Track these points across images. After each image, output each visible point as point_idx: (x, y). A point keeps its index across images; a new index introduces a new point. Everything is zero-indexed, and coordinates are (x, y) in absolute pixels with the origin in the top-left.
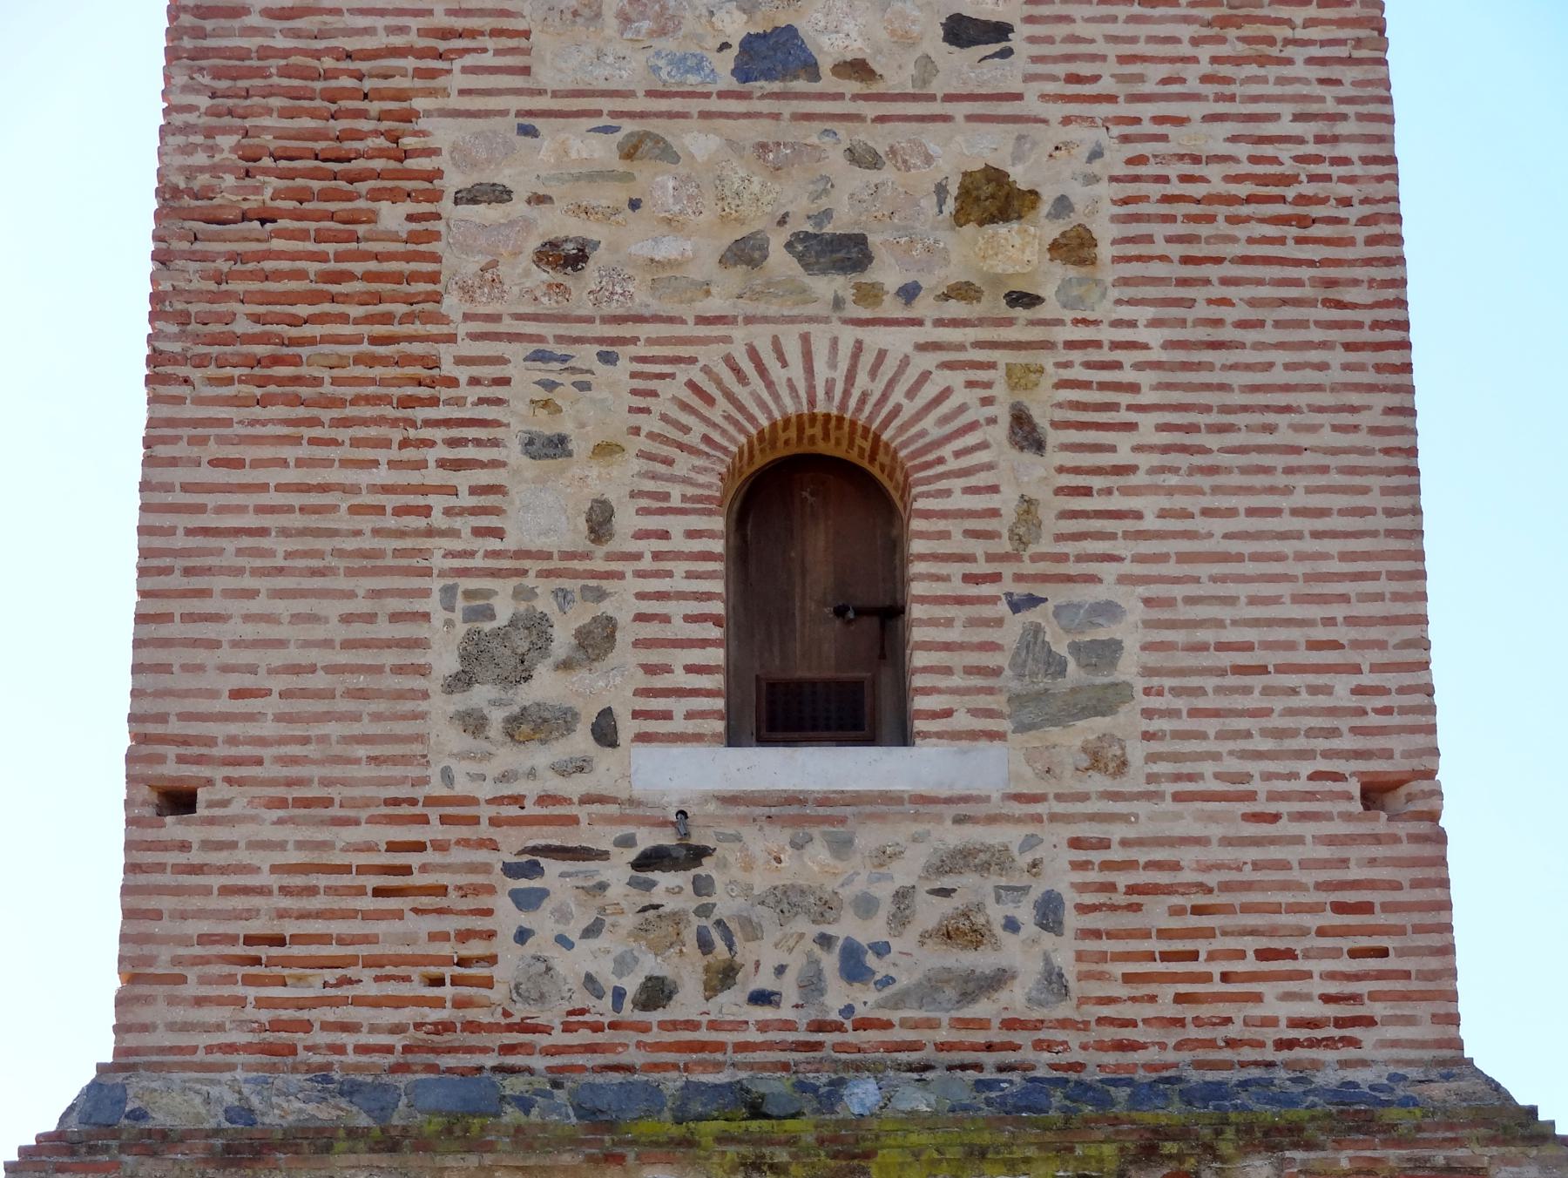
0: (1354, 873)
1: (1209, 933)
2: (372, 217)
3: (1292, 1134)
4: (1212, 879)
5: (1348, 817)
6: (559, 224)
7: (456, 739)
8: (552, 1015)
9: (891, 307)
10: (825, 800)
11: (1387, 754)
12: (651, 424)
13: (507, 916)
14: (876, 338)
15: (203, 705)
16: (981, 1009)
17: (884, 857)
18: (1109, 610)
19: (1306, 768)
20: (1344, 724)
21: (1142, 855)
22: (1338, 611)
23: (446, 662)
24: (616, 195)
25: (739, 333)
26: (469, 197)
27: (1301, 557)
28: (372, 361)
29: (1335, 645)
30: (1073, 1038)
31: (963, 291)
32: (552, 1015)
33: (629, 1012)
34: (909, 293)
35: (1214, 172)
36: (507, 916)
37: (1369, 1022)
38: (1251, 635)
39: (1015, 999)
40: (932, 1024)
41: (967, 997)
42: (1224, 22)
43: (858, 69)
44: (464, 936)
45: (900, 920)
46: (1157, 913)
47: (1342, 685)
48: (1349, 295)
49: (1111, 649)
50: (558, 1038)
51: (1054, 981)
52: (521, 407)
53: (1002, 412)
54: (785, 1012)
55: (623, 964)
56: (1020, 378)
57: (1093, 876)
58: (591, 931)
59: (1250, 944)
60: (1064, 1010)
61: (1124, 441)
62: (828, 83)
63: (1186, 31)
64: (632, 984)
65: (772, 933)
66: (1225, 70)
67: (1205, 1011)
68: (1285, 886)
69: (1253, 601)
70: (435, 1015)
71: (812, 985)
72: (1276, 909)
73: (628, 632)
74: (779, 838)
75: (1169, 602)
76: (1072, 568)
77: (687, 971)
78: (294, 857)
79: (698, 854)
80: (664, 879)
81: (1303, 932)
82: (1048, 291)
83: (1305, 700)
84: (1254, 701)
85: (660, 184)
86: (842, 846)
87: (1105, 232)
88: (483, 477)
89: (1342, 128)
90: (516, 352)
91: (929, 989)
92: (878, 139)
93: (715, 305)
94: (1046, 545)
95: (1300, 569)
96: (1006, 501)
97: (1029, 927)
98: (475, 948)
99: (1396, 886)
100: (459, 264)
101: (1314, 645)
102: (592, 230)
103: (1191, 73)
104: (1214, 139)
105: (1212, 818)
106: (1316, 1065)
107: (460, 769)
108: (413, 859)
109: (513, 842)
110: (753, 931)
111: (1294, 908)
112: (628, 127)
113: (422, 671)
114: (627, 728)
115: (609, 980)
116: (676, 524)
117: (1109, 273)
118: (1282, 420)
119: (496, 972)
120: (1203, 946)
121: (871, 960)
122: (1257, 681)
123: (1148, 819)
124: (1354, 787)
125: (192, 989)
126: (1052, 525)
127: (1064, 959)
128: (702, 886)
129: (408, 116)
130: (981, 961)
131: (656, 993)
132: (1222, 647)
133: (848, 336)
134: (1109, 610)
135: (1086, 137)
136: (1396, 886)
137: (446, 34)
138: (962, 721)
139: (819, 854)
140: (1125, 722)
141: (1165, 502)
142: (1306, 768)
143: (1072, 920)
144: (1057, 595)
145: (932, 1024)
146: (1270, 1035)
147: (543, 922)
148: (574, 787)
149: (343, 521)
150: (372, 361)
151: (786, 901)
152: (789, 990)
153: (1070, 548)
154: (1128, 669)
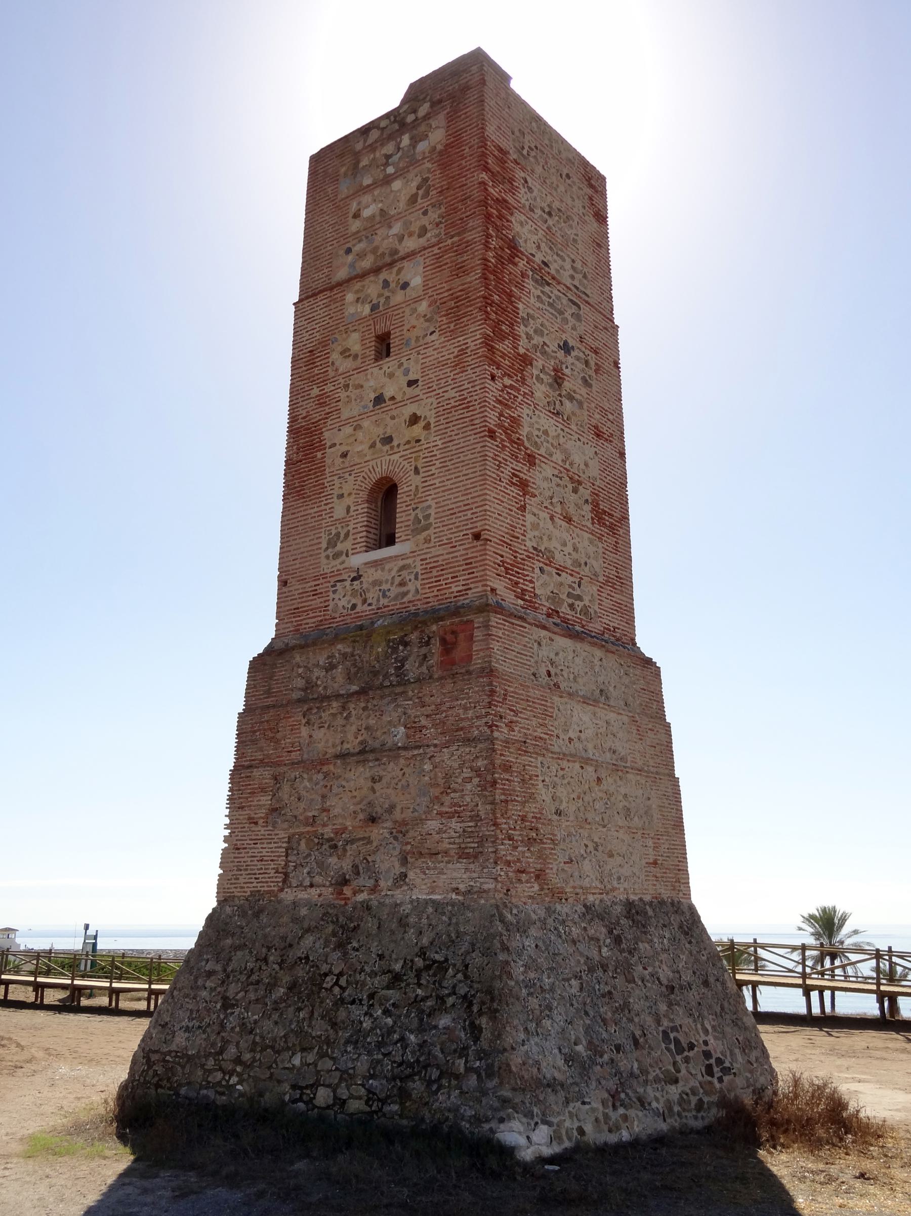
0: (470, 556)
1: (443, 575)
2: (316, 456)
3: (442, 619)
4: (444, 563)
5: (469, 543)
6: (344, 448)
7: (324, 561)
8: (337, 615)
9: (396, 450)
10: (381, 560)
11: (476, 527)
12: (356, 487)
13: (332, 596)
14: (392, 458)
15: (288, 564)
16: (405, 599)
17: (390, 570)
18: (429, 507)
19: (462, 534)
20: (469, 522)
21: (432, 560)
22: (470, 496)
23: (324, 545)
24: (352, 439)
25: (370, 463)
26: (330, 447)
27: (463, 486)
28: (315, 486)
29: (468, 504)
30: (419, 603)
31: (408, 442)
32: (337, 615)
33: (350, 612)
34: (399, 446)
35: (452, 401)
36: (332, 596)
37: (470, 589)
38: (454, 506)
39: (410, 597)
40: (396, 605)
41: (403, 598)
42: (456, 365)
43: (393, 398)
44: (325, 601)
45: (392, 584)
46: (435, 573)
47: (469, 513)
48: (476, 422)
49: (427, 517)
50: (338, 619)
51: (417, 591)
52: (336, 489)
53: (413, 468)
54: (373, 607)
55: (349, 602)
56: (416, 459)
57: (424, 567)
58: (344, 596)
59: (450, 576)
60: (419, 597)
61: (433, 468)
62: (388, 403)
63: (448, 370)
64: (349, 606)
65: (372, 590)
66: (456, 377)
67: (442, 592)
68: (457, 561)
69: (455, 498)
70: (320, 619)
71: (378, 600)
72: (455, 567)
73: (352, 532)
74: (373, 570)
75: (439, 502)
76: (423, 499)
77: (358, 601)
78: (301, 591)
79: (360, 576)
80: (355, 583)
81: (459, 571)
82: (422, 438)
83: (463, 518)
84: (453, 521)
85: (360, 435)
86: (383, 570)
87: (432, 421)
88: (330, 506)
89: (476, 383)
90: (335, 478)
91: (396, 598)
92: (394, 413)
93: (367, 458)
94: (419, 495)
95: (463, 488)
96: (413, 488)
97: (413, 580)
98: (326, 604)
99: (476, 557)
100: (328, 461)
101: (465, 505)
102: (348, 448)
103: (449, 379)
104: (452, 393)
105: (444, 549)
106: (459, 601)
107: (326, 567)
108: (317, 588)
109: (333, 580)
110: (369, 592)
111: (458, 566)
112: (355, 424)
113: (320, 548)
114: (350, 552)
115: (347, 606)
116: (359, 507)
117: (433, 430)
118: (461, 455)
119: (329, 608)
120: (442, 578)
121: (387, 593)
122: (454, 516)
123: (435, 551)
124: (470, 536)
125: (286, 621)
126: (421, 490)
127: (419, 587)
128: (361, 583)
129: (322, 433)
130: (404, 589)
131: (354, 607)
132: (449, 510)
133: (388, 458)
134: (429, 507)
135: (430, 400)
136: (476, 557)
137: (328, 413)
138: (404, 538)
139: (379, 572)
140: (431, 531)
141: (440, 480)
142: (462, 534)
143: (420, 577)
144: (421, 506)
145: (396, 605)
146: (453, 595)
147: (336, 596)
148: (341, 567)
149: (309, 521)
150: (315, 486)
151: (376, 583)
152: (375, 602)
153: (424, 495)
154: (432, 520)
